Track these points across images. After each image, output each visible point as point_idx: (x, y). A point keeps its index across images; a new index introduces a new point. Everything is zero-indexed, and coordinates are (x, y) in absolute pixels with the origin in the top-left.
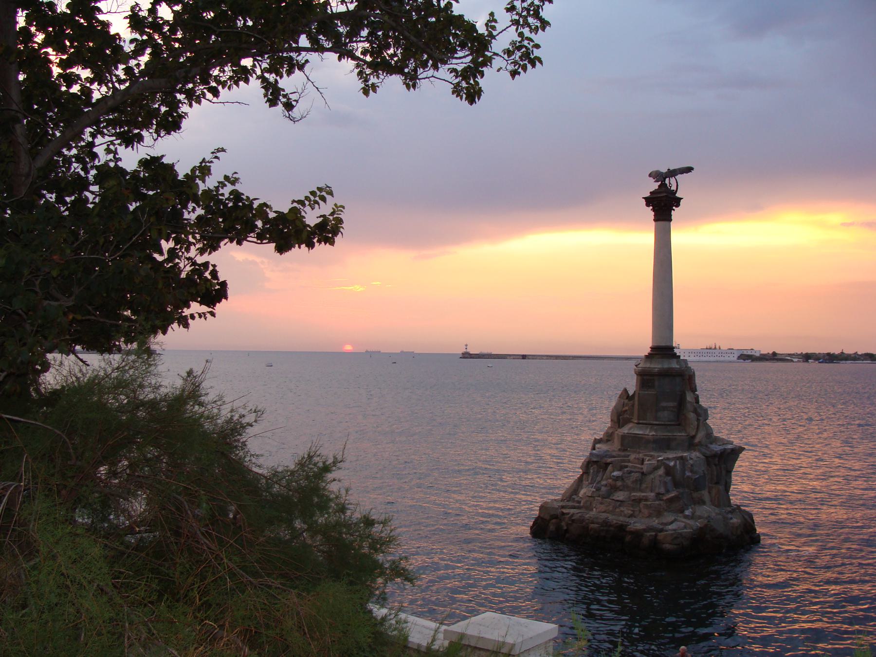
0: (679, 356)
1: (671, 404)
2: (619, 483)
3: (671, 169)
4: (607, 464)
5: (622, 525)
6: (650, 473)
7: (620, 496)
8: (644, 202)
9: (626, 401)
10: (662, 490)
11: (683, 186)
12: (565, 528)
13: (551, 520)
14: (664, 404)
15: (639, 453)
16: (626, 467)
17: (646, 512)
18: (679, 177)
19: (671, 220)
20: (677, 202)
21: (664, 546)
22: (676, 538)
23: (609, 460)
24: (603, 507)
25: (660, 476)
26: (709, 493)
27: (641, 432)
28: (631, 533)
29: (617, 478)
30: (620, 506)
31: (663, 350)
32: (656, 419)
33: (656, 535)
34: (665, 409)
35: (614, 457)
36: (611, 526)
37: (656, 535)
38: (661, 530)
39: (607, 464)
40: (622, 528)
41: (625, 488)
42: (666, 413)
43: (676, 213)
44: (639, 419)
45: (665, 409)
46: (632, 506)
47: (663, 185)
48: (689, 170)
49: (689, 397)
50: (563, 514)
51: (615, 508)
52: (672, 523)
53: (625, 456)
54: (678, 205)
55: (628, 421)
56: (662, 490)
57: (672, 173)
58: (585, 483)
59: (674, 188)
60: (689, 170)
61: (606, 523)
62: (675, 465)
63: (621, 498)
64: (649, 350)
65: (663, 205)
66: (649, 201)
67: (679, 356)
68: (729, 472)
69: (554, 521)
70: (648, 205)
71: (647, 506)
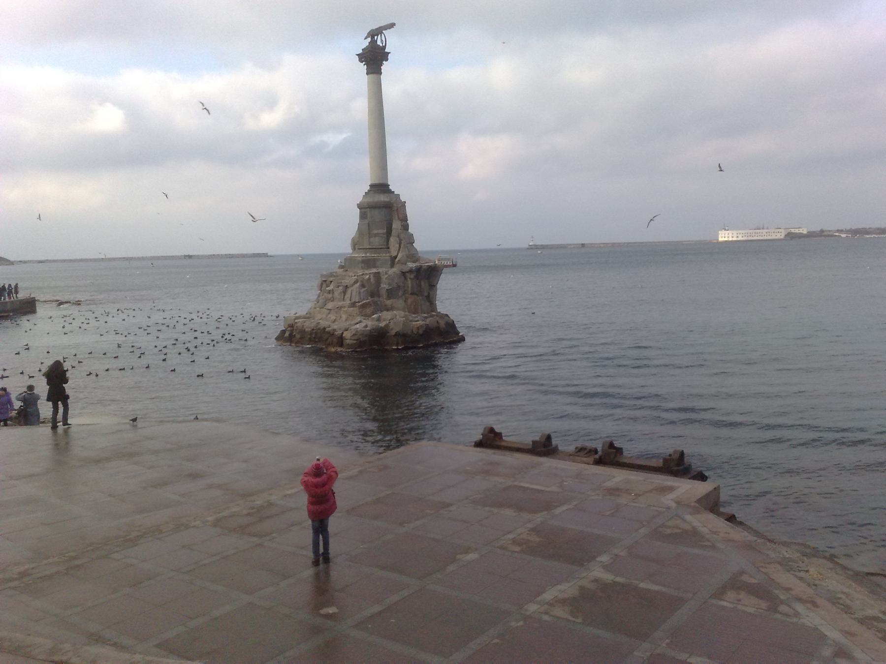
1: (381, 231)
7: (330, 305)
14: (375, 232)
22: (354, 335)
23: (331, 279)
28: (328, 333)
31: (381, 188)
34: (376, 235)
42: (377, 239)
43: (385, 67)
45: (376, 235)
47: (373, 42)
48: (392, 26)
49: (396, 225)
60: (392, 26)
62: (369, 279)
64: (369, 188)
65: (374, 58)
66: (362, 57)
68: (433, 287)
71: (346, 312)
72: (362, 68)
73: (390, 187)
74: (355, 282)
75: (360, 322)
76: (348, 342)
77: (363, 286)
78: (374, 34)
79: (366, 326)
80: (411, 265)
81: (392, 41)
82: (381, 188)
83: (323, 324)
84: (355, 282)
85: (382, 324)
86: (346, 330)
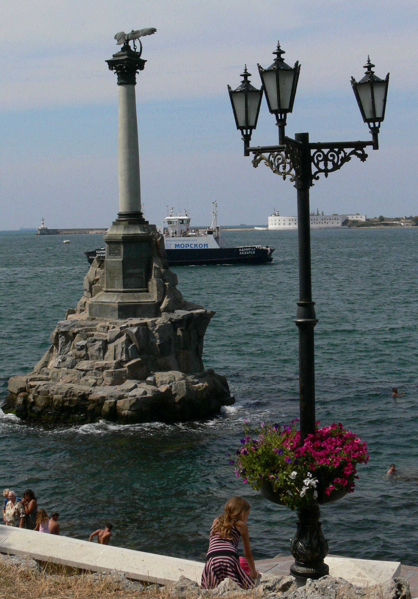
0: (148, 222)
1: (137, 271)
2: (83, 352)
3: (135, 30)
4: (75, 334)
7: (84, 365)
8: (107, 65)
12: (32, 400)
13: (18, 393)
14: (131, 271)
15: (106, 321)
16: (92, 335)
17: (109, 379)
18: (142, 38)
19: (135, 83)
20: (141, 65)
21: (123, 412)
23: (76, 330)
24: (68, 378)
26: (177, 358)
27: (108, 300)
28: (93, 401)
29: (82, 348)
30: (84, 375)
33: (116, 402)
36: (74, 395)
37: (116, 402)
39: (75, 334)
40: (84, 397)
41: (87, 357)
43: (140, 76)
44: (107, 288)
46: (96, 374)
47: (126, 48)
48: (152, 31)
52: (132, 389)
53: (92, 325)
54: (142, 68)
55: (99, 290)
57: (135, 35)
58: (55, 353)
59: (138, 50)
60: (152, 31)
61: (69, 393)
63: (85, 368)
66: (112, 64)
67: (148, 222)
68: (200, 338)
69: (21, 394)
70: (111, 68)
72: (113, 76)
73: (144, 216)
74: (119, 336)
75: (136, 387)
76: (126, 412)
77: (129, 341)
78: (125, 39)
79: (145, 393)
80: (180, 313)
81: (148, 49)
82: (134, 216)
83: (80, 388)
84: (119, 336)
85: (163, 389)
86: (121, 397)
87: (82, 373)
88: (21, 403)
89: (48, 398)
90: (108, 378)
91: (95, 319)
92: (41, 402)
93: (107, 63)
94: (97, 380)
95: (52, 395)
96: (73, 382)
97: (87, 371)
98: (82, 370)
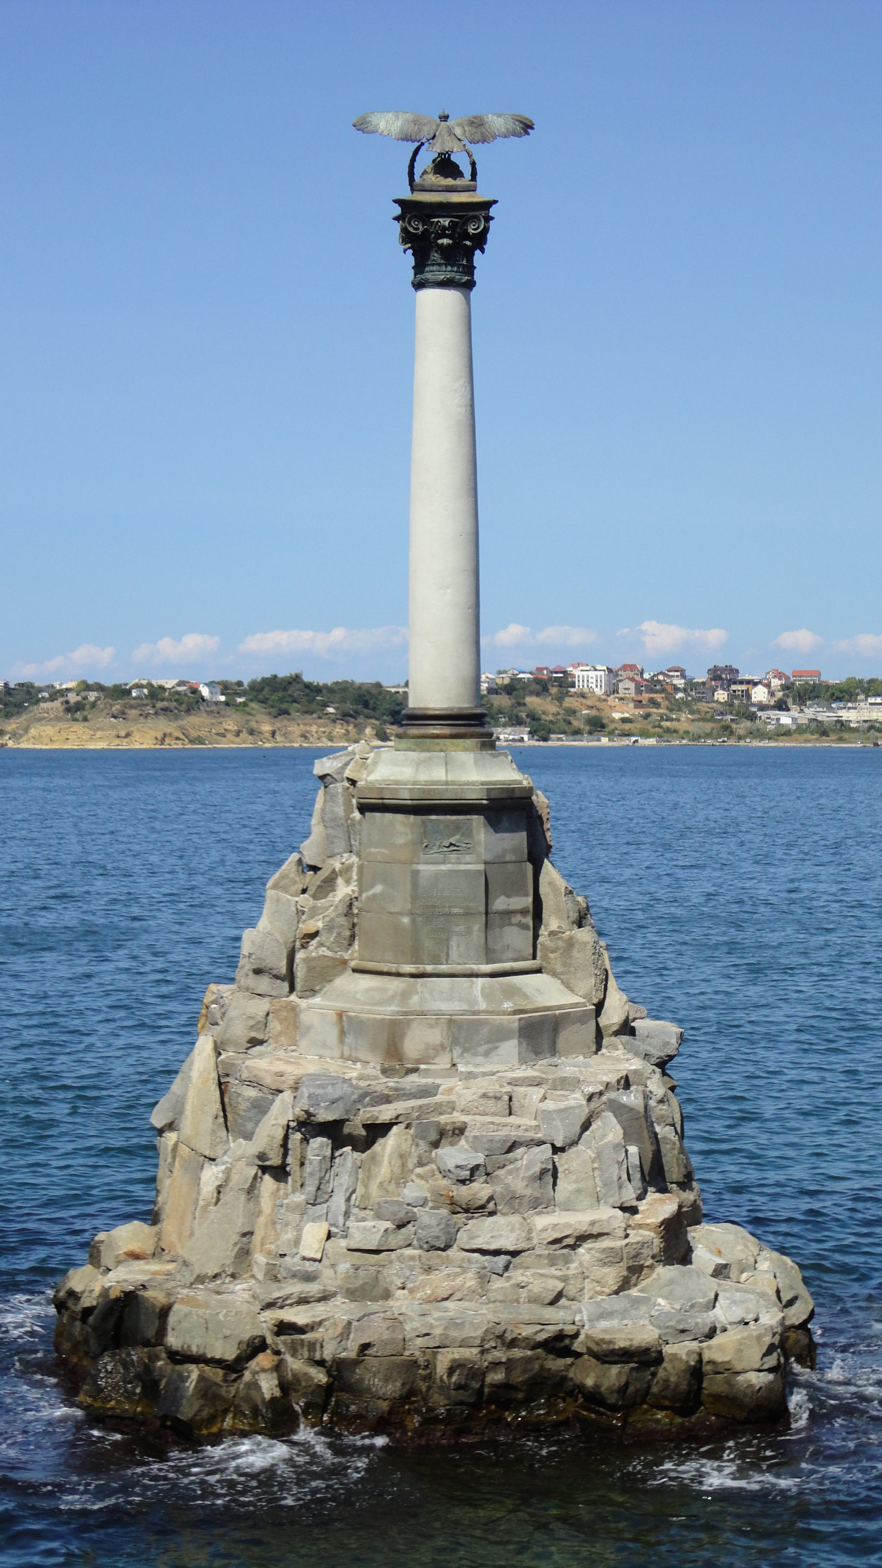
5: (560, 1336)
6: (575, 1143)
9: (305, 900)
10: (629, 1194)
11: (497, 177)
14: (500, 903)
17: (612, 1275)
23: (385, 1113)
25: (616, 1147)
28: (609, 1356)
32: (490, 955)
35: (387, 1100)
38: (711, 1333)
46: (552, 1261)
50: (283, 1328)
51: (484, 1278)
54: (480, 241)
56: (629, 1194)
69: (264, 1360)
87: (502, 1259)
88: (277, 1393)
89: (414, 1364)
90: (606, 1270)
91: (415, 1070)
92: (386, 1380)
93: (397, 210)
94: (564, 1279)
95: (424, 1350)
96: (458, 1295)
97: (515, 1254)
98: (496, 1253)
